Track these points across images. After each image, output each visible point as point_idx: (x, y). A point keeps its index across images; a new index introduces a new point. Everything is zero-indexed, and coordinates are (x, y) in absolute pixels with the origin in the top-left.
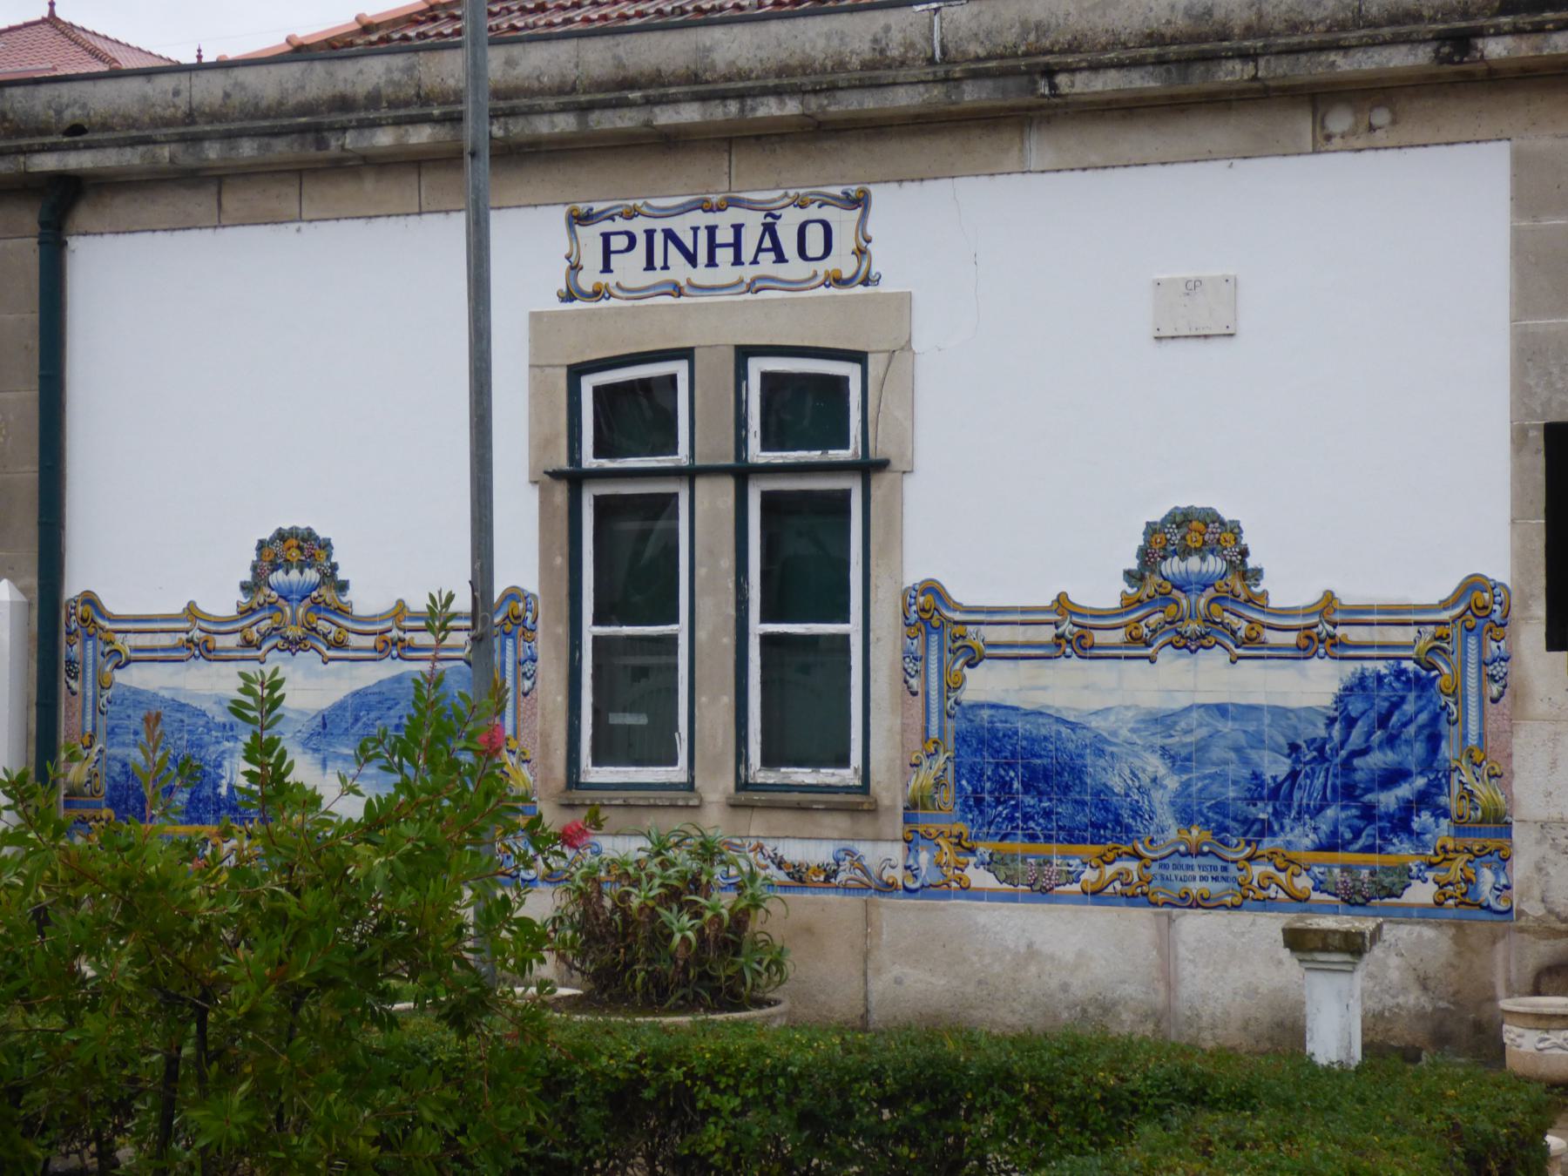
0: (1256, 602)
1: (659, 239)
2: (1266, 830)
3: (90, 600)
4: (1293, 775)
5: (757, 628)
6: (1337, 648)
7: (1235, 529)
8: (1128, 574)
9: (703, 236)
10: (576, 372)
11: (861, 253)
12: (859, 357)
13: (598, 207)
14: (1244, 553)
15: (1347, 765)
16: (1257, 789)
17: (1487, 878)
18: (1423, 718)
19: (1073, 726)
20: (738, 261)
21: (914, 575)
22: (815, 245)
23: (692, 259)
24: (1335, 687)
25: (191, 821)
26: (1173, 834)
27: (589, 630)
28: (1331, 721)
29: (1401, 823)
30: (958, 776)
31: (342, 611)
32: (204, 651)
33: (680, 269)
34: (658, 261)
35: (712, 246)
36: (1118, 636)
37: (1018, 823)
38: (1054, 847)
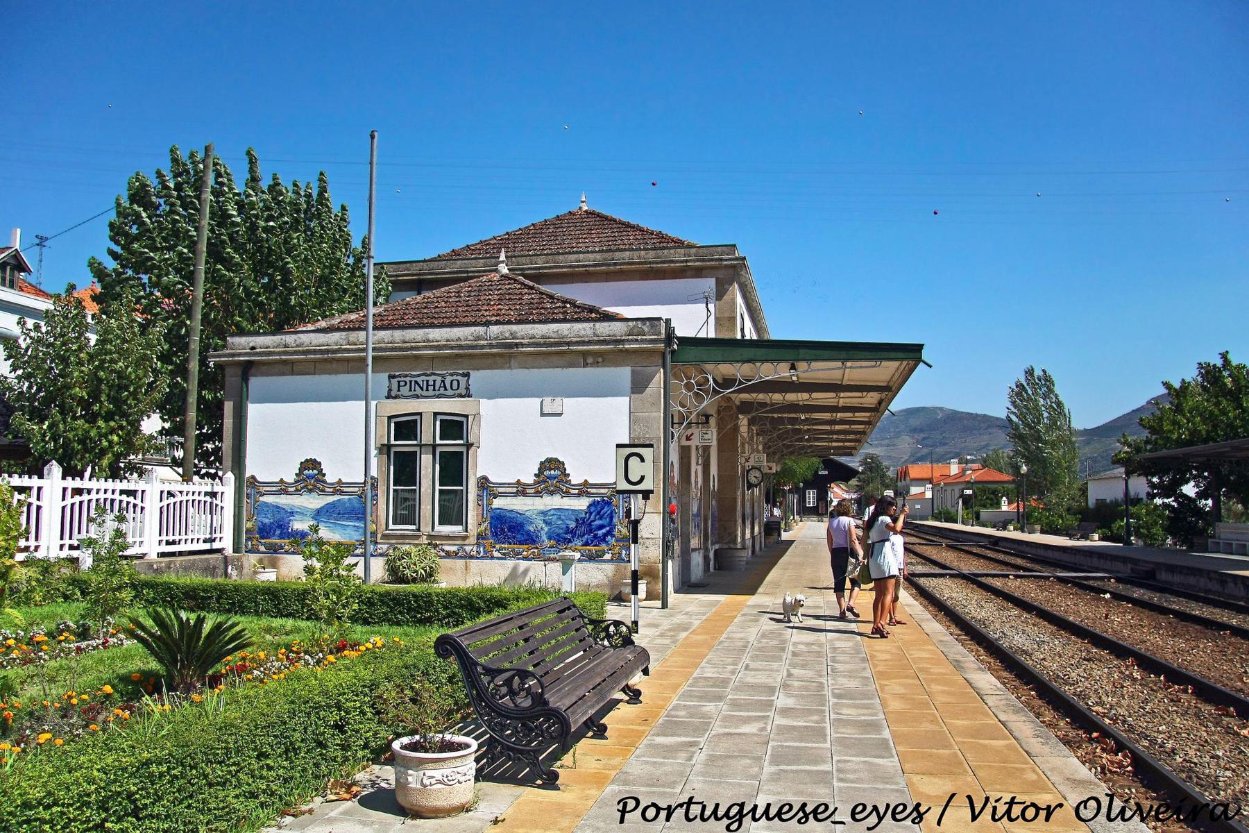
0: (568, 482)
1: (413, 383)
2: (570, 541)
3: (253, 477)
4: (577, 527)
5: (438, 487)
6: (588, 494)
7: (563, 463)
8: (535, 475)
9: (425, 383)
10: (390, 418)
11: (467, 389)
12: (467, 416)
13: (397, 374)
14: (565, 470)
16: (568, 530)
17: (624, 552)
18: (609, 512)
19: (520, 514)
20: (434, 390)
21: (479, 474)
23: (422, 389)
24: (587, 504)
25: (280, 539)
27: (392, 487)
28: (586, 513)
29: (603, 539)
30: (491, 528)
31: (325, 482)
33: (419, 391)
34: (413, 389)
35: (428, 385)
36: (533, 491)
38: (516, 546)
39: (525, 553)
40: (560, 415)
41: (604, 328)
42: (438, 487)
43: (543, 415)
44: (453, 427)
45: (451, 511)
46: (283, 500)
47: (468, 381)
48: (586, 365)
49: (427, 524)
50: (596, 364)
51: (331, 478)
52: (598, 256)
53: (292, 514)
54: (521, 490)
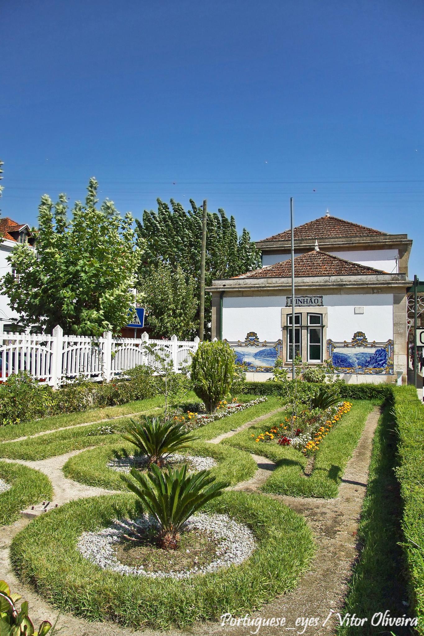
2: (367, 366)
3: (226, 340)
7: (364, 334)
10: (287, 315)
11: (322, 303)
12: (322, 314)
15: (376, 359)
16: (366, 362)
17: (391, 371)
21: (328, 339)
22: (316, 302)
23: (302, 303)
26: (357, 367)
27: (289, 344)
29: (382, 365)
31: (258, 342)
32: (241, 346)
33: (300, 304)
35: (304, 301)
37: (340, 365)
39: (348, 371)
40: (363, 314)
41: (381, 278)
42: (309, 344)
43: (355, 314)
44: (316, 319)
45: (315, 353)
46: (239, 349)
47: (322, 299)
48: (374, 293)
49: (305, 359)
50: (378, 293)
51: (261, 340)
52: (344, 240)
53: (244, 355)
54: (346, 345)
